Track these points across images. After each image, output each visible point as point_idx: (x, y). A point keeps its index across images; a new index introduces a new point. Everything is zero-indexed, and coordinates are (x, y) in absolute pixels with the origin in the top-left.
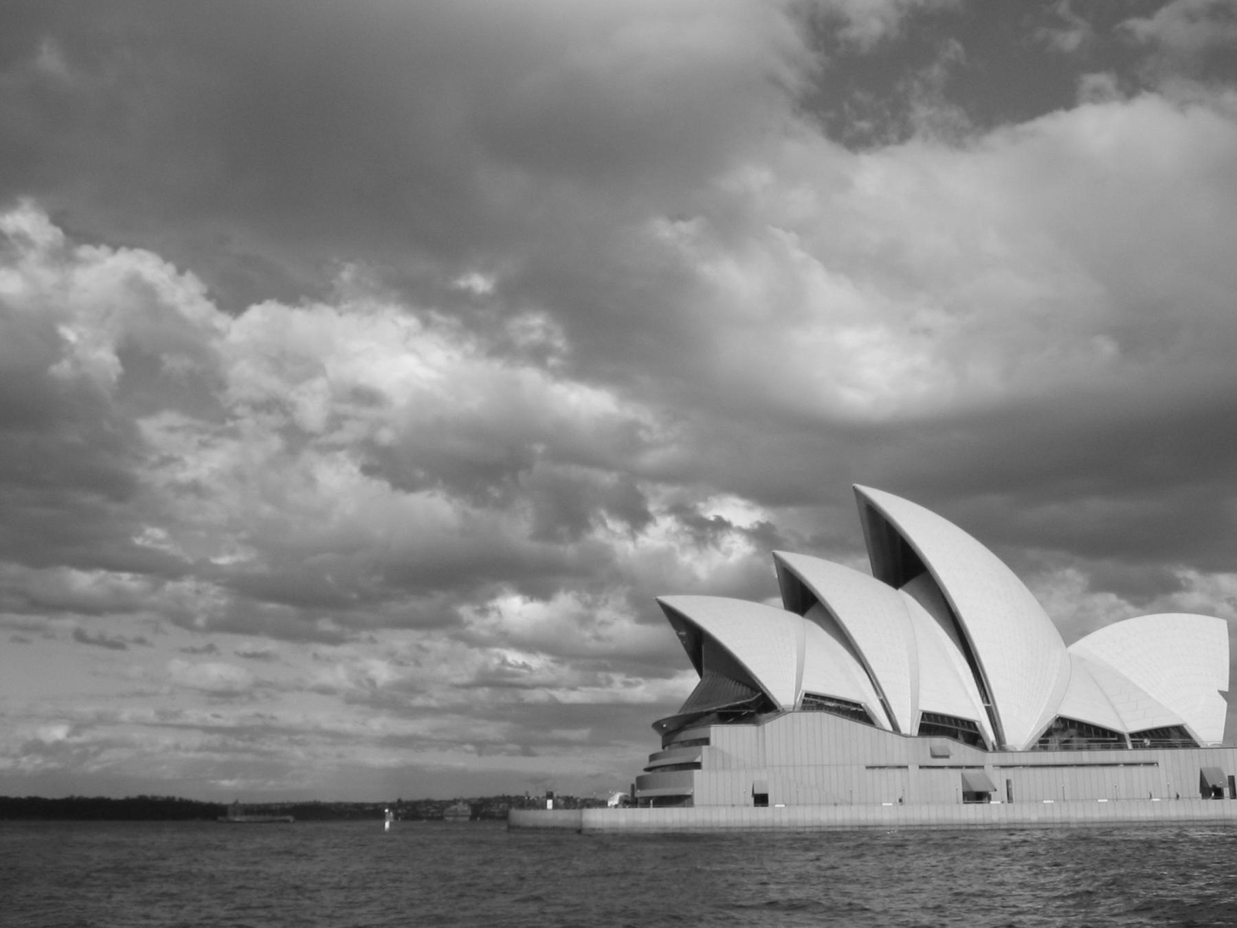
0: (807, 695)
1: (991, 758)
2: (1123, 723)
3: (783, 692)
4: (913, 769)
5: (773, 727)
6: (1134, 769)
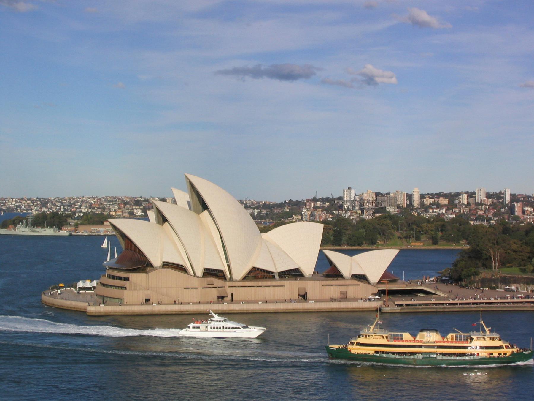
0: (164, 262)
1: (228, 284)
2: (276, 269)
3: (156, 261)
4: (200, 289)
5: (152, 275)
6: (276, 288)
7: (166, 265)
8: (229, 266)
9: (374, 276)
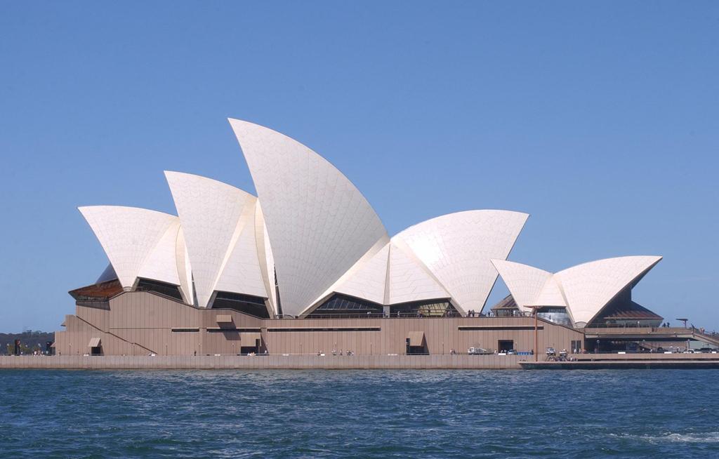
1: (268, 324)
7: (145, 285)
8: (277, 289)
9: (583, 313)
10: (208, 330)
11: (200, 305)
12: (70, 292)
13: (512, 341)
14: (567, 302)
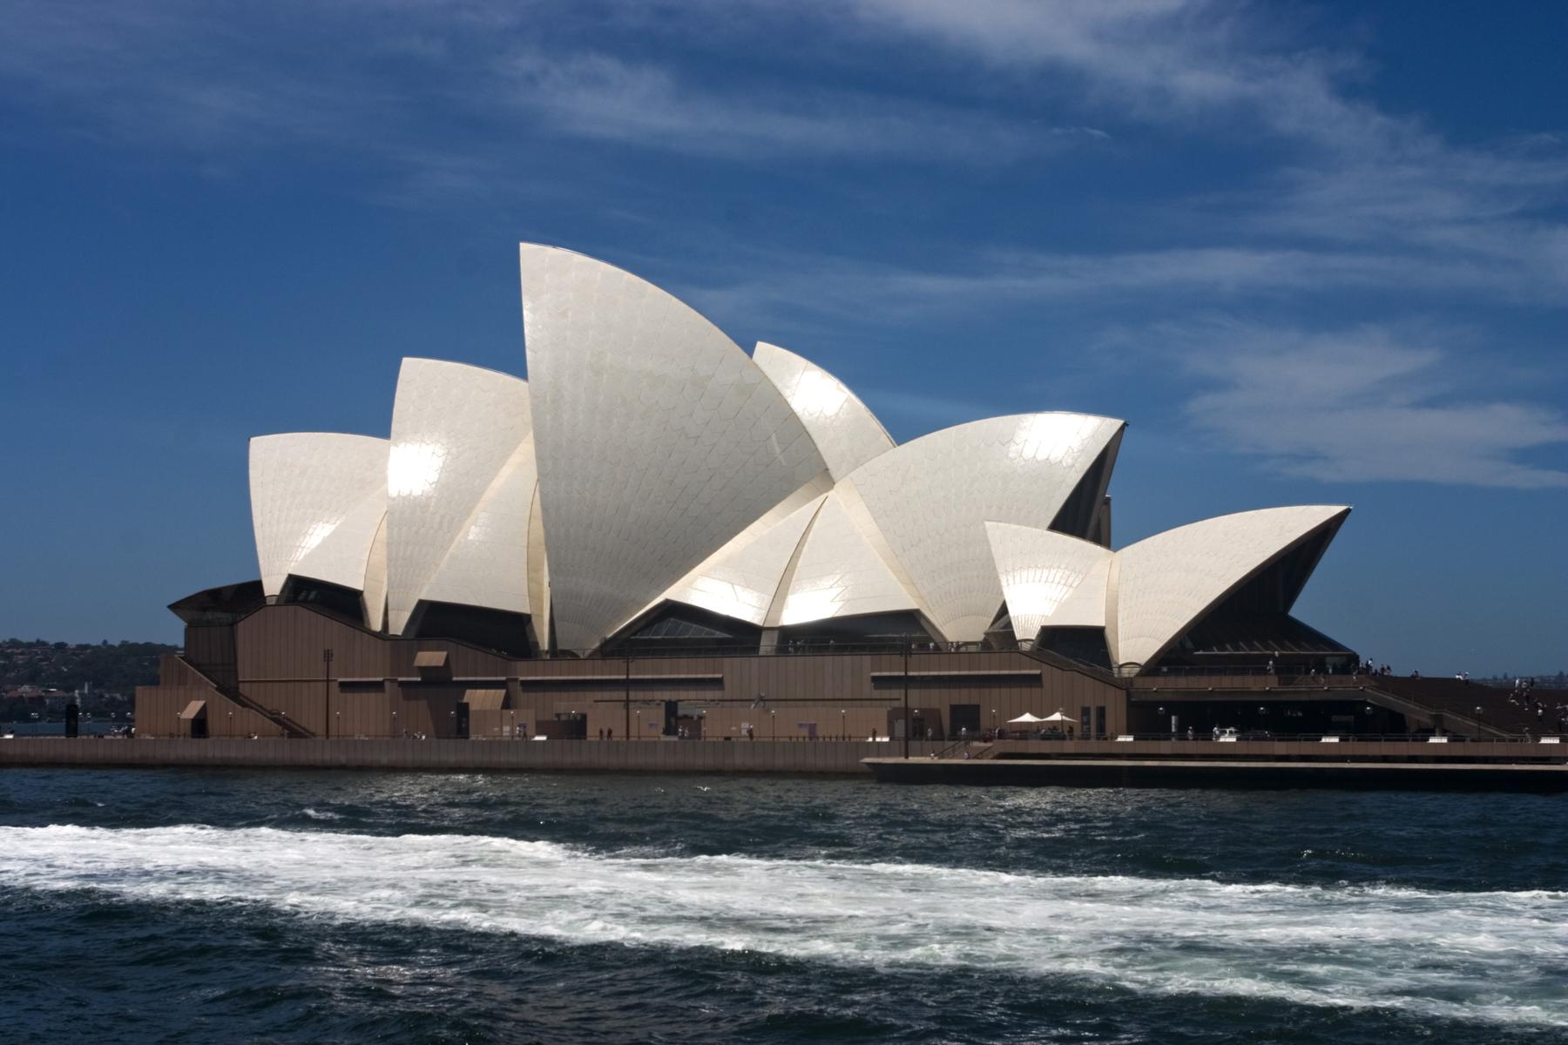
5: (247, 629)
10: (401, 684)
11: (392, 632)
12: (174, 607)
13: (978, 707)
14: (1112, 613)
